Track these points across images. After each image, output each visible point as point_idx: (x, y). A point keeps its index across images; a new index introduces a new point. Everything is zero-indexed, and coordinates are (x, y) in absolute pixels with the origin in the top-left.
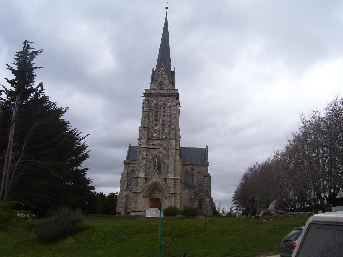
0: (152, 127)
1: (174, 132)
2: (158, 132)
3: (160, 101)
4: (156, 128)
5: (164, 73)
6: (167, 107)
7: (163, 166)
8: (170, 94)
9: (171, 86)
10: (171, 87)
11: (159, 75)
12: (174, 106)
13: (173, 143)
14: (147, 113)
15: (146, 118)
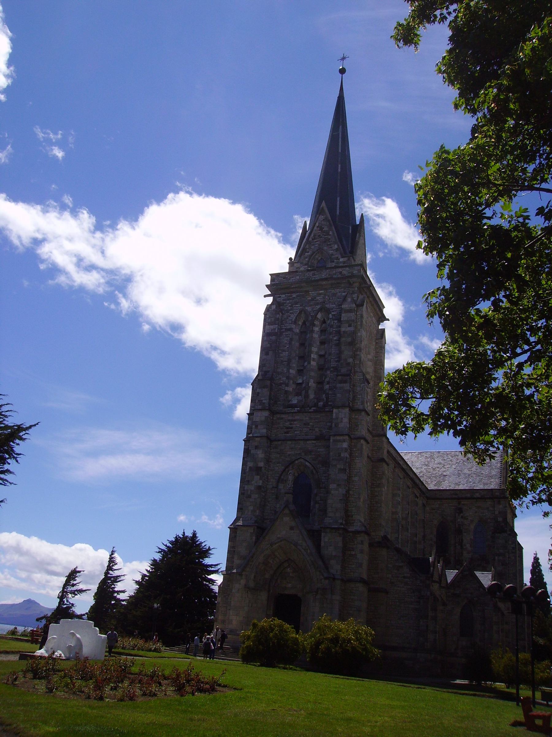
0: (288, 378)
1: (347, 386)
2: (303, 392)
3: (312, 303)
4: (300, 381)
5: (326, 229)
6: (330, 316)
7: (315, 491)
8: (338, 278)
9: (345, 259)
10: (344, 262)
11: (312, 235)
12: (350, 311)
13: (342, 419)
14: (274, 338)
15: (271, 353)
